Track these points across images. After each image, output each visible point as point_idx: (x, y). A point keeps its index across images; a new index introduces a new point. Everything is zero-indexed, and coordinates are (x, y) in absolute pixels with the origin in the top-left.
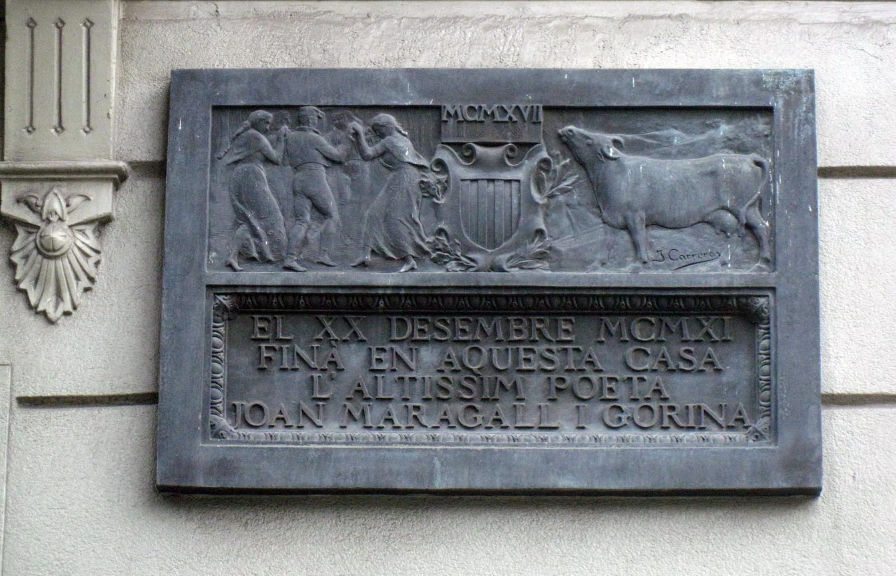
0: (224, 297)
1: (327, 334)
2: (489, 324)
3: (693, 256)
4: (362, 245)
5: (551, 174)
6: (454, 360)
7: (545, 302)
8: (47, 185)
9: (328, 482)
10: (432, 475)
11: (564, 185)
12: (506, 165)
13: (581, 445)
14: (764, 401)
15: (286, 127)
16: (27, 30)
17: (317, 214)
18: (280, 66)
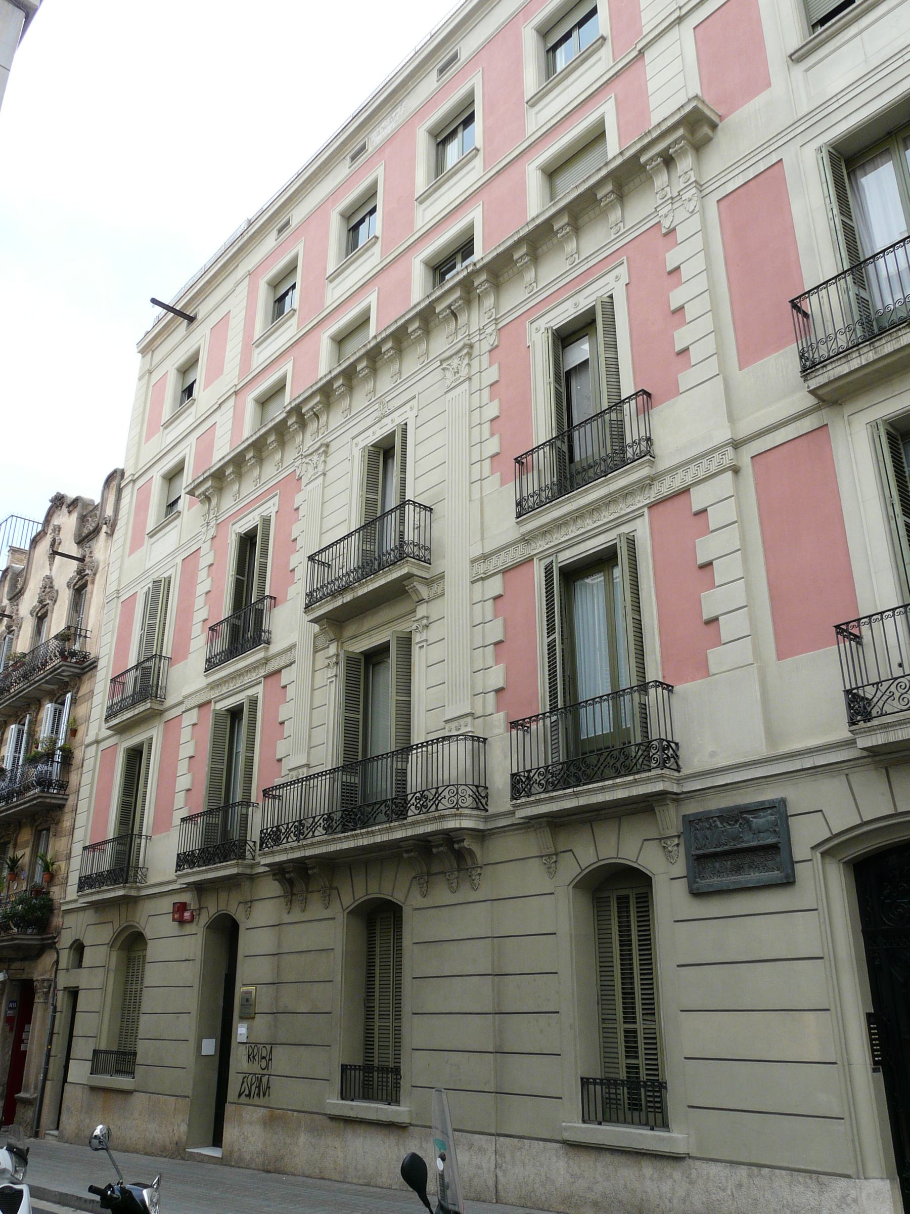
9: (714, 890)
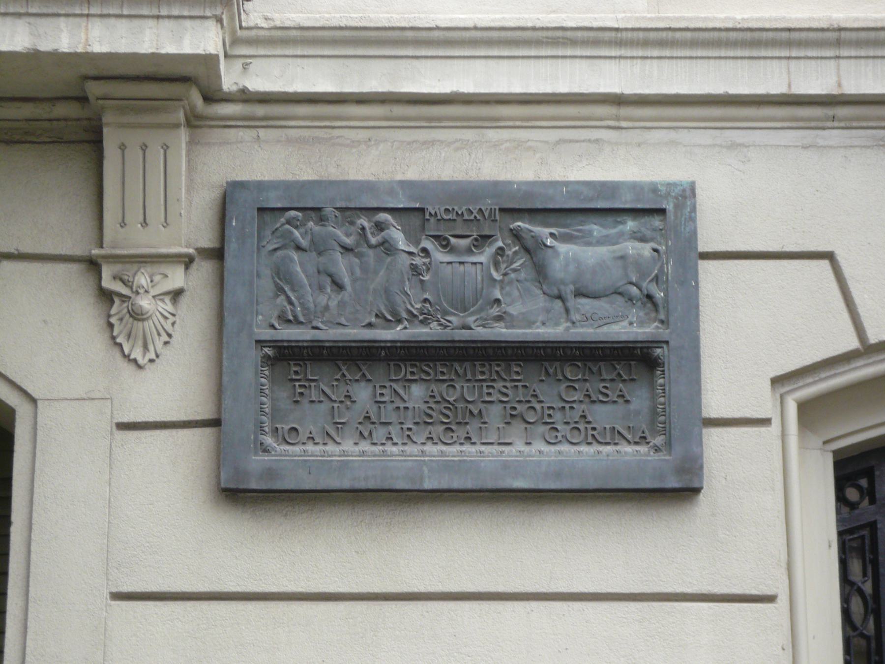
0: (268, 348)
1: (344, 375)
2: (461, 367)
3: (609, 317)
4: (369, 310)
5: (505, 258)
6: (436, 394)
7: (502, 352)
8: (135, 267)
9: (346, 484)
10: (422, 478)
11: (514, 266)
12: (473, 251)
13: (530, 456)
14: (660, 423)
15: (312, 223)
16: (119, 151)
17: (335, 288)
18: (305, 177)
